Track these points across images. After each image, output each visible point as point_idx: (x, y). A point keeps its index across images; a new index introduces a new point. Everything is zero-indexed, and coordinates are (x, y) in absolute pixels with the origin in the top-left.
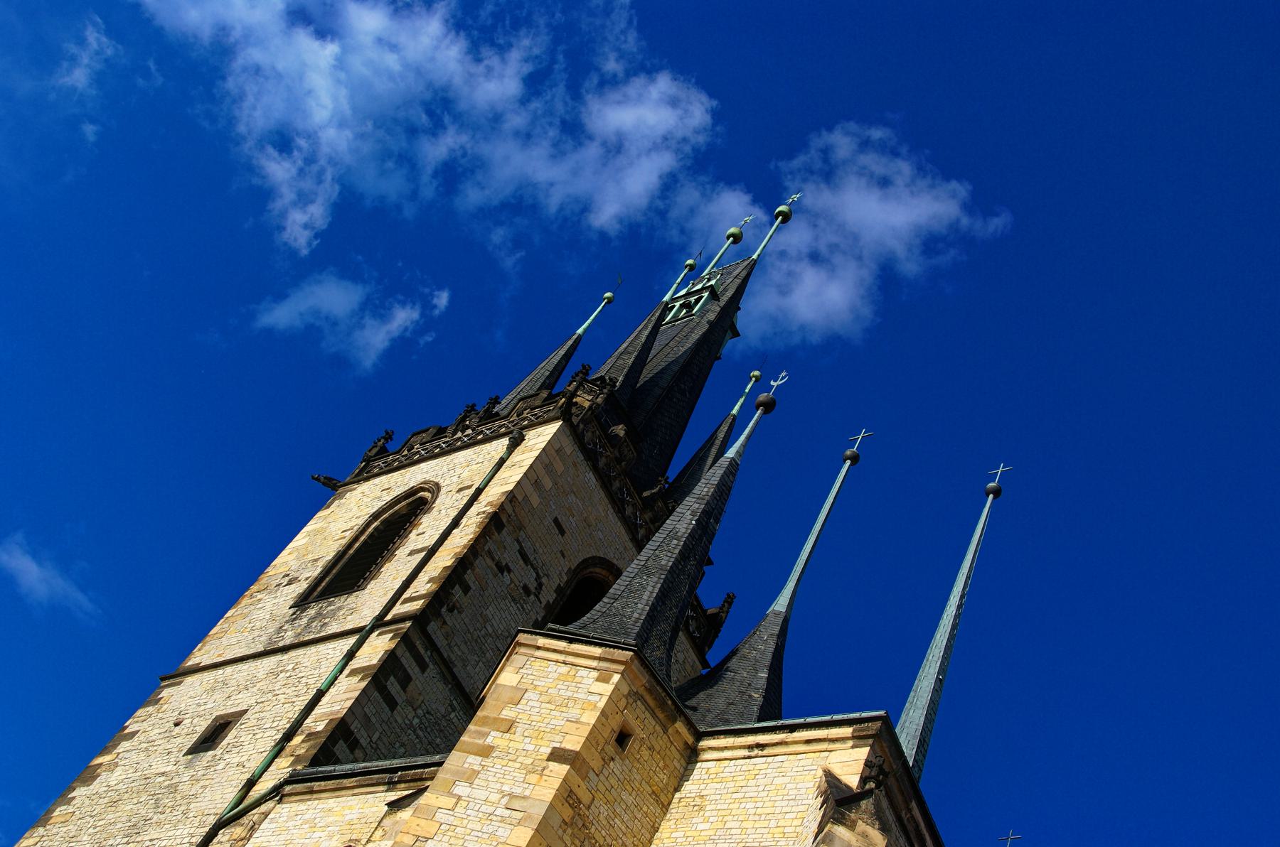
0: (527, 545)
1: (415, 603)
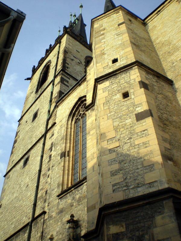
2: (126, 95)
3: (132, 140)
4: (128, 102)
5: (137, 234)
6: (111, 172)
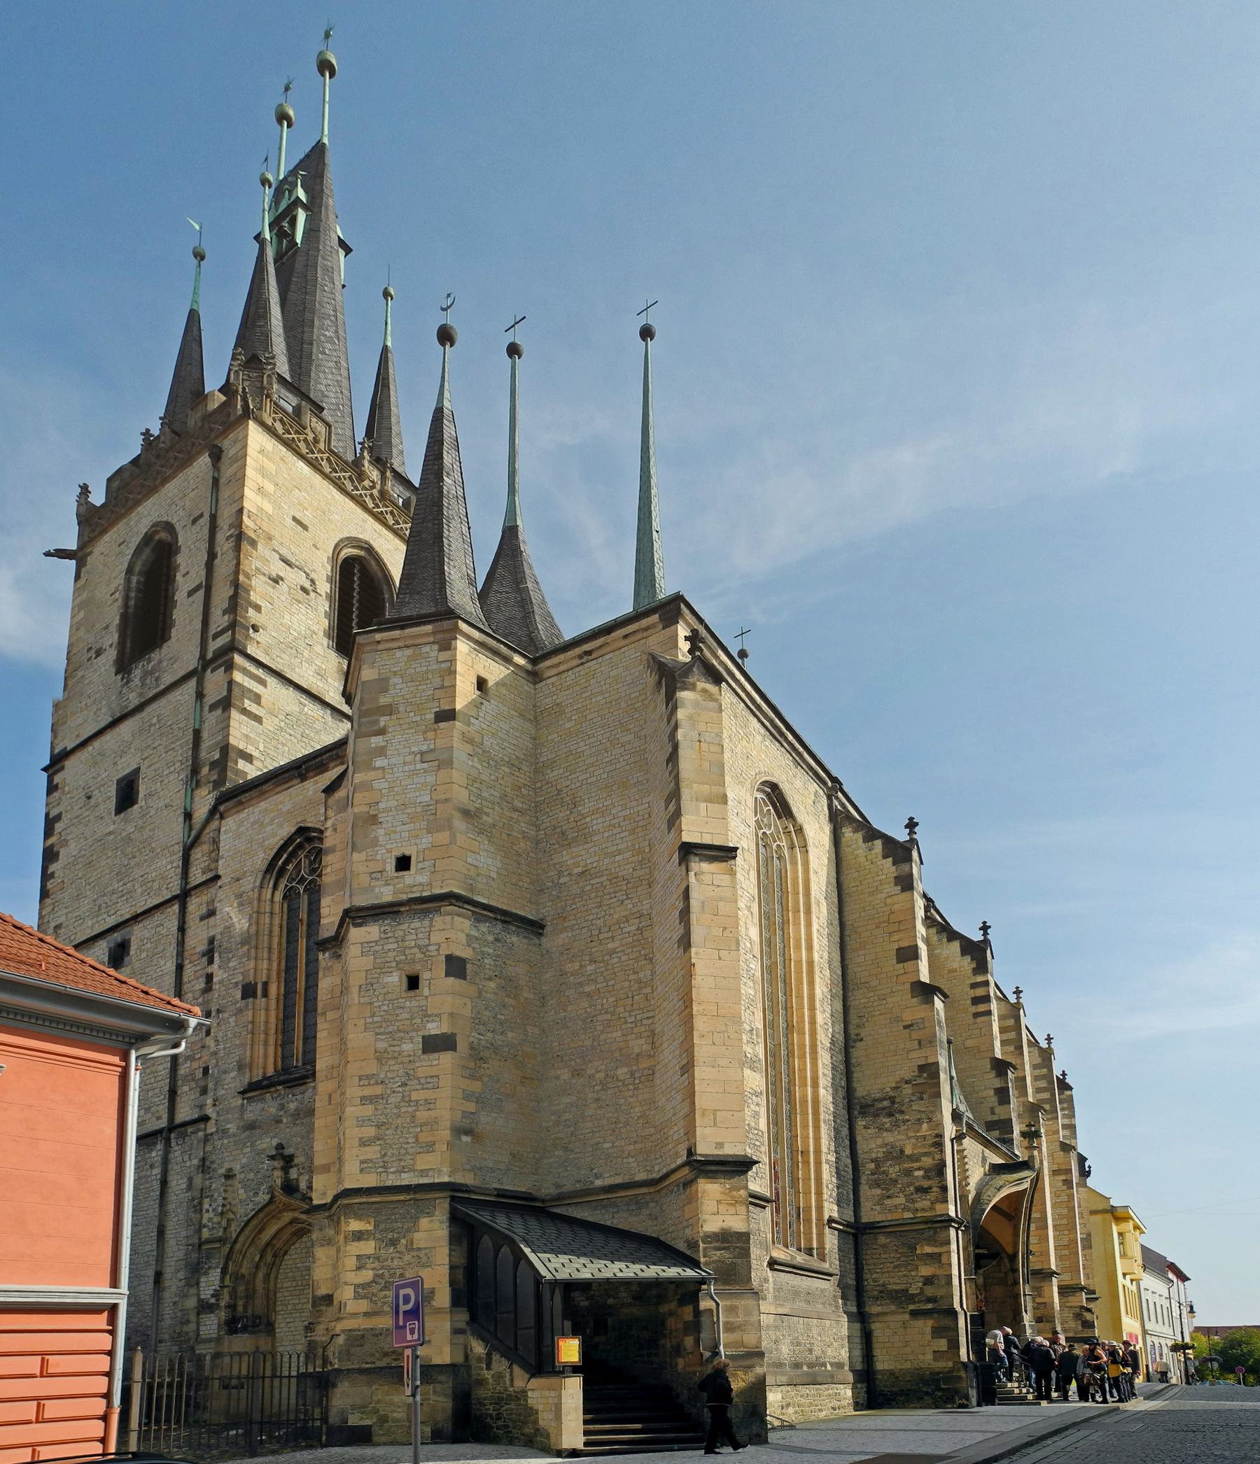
0: (284, 552)
1: (225, 635)
2: (413, 983)
3: (407, 1088)
4: (412, 1002)
5: (390, 1236)
6: (360, 1139)
